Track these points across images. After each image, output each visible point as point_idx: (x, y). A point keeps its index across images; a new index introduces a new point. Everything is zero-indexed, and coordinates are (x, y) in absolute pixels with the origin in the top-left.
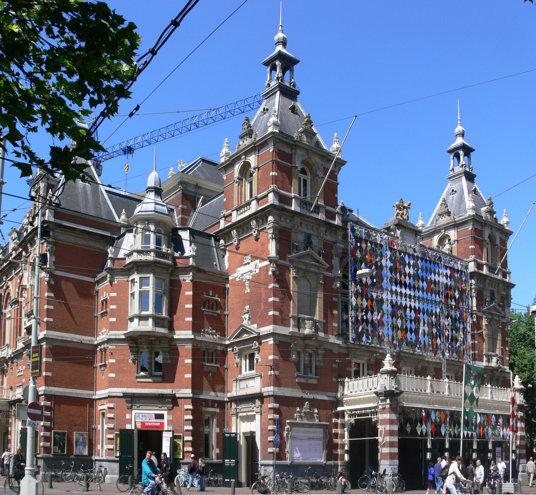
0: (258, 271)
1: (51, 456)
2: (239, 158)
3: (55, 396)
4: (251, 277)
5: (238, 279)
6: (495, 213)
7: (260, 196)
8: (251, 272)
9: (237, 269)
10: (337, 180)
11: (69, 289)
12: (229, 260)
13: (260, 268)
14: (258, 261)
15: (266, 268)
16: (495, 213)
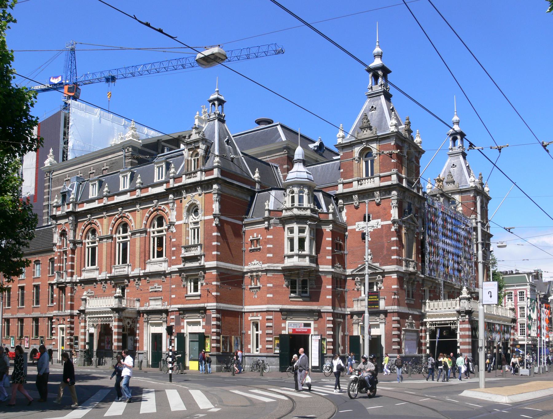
0: (379, 227)
1: (220, 353)
2: (361, 143)
3: (222, 310)
4: (372, 230)
5: (357, 230)
6: (412, 132)
7: (382, 174)
8: (373, 227)
9: (357, 223)
10: (419, 164)
11: (227, 228)
12: (347, 214)
13: (382, 226)
14: (380, 220)
15: (389, 226)
16: (412, 132)
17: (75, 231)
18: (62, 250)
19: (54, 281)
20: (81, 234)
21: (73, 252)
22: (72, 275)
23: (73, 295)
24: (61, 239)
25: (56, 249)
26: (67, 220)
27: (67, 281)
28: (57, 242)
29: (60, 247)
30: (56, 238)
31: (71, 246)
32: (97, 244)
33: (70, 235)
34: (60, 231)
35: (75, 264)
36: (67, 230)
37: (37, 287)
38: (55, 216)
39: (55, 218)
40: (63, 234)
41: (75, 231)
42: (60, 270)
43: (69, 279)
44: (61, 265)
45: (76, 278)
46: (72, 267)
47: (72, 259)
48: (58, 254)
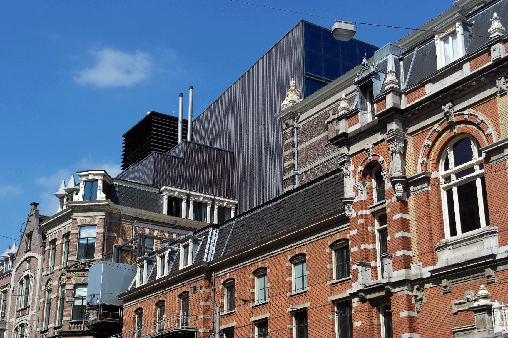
17: (403, 156)
18: (368, 212)
19: (356, 287)
20: (422, 159)
22: (406, 262)
23: (415, 314)
25: (351, 212)
27: (393, 280)
28: (353, 195)
29: (362, 205)
30: (351, 186)
31: (399, 188)
32: (478, 171)
33: (393, 167)
34: (361, 168)
35: (412, 235)
36: (381, 159)
37: (301, 315)
38: (345, 134)
39: (344, 140)
40: (373, 170)
41: (403, 156)
42: (367, 258)
43: (399, 275)
44: (370, 247)
45: (419, 270)
46: (406, 244)
47: (404, 225)
48: (361, 221)
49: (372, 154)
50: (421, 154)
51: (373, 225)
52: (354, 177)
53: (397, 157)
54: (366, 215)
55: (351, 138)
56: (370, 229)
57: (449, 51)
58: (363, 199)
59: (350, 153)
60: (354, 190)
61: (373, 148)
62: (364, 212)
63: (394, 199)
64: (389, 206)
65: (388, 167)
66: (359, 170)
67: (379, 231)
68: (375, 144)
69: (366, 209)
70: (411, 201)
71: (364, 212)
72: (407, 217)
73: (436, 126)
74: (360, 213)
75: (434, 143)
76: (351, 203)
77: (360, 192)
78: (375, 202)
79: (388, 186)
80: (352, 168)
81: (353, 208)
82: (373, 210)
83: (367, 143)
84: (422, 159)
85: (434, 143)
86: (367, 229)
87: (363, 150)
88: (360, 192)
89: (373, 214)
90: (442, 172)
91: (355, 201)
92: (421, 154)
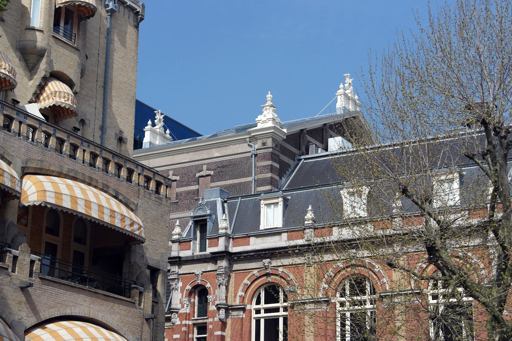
18: (191, 323)
20: (240, 293)
21: (223, 325)
24: (189, 301)
26: (210, 267)
28: (179, 306)
34: (189, 287)
36: (208, 285)
38: (180, 258)
40: (201, 292)
48: (184, 329)
49: (200, 279)
50: (241, 288)
51: (193, 333)
52: (182, 292)
53: (223, 288)
54: (189, 325)
55: (183, 261)
56: (190, 336)
57: (272, 216)
58: (188, 312)
59: (181, 272)
60: (181, 303)
61: (202, 274)
62: (187, 322)
63: (216, 319)
64: (211, 323)
65: (214, 294)
66: (187, 288)
67: (197, 338)
68: (203, 272)
69: (189, 320)
70: (229, 322)
71: (187, 322)
72: (224, 334)
73: (255, 272)
74: (184, 322)
75: (252, 283)
76: (177, 313)
77: (185, 306)
78: (196, 317)
79: (212, 308)
80: (180, 284)
81: (178, 317)
82: (195, 322)
83: (198, 269)
84: (240, 293)
85: (252, 283)
86: (188, 336)
87: (193, 273)
88: (185, 306)
89: (194, 325)
90: (254, 306)
91: (180, 311)
92: (241, 288)
